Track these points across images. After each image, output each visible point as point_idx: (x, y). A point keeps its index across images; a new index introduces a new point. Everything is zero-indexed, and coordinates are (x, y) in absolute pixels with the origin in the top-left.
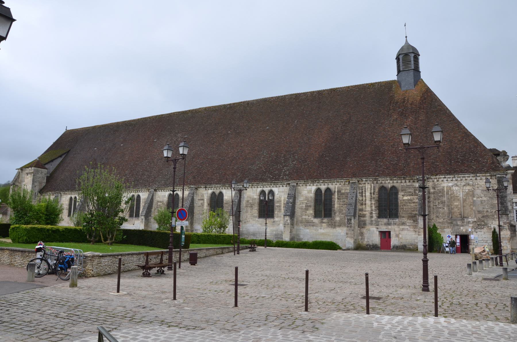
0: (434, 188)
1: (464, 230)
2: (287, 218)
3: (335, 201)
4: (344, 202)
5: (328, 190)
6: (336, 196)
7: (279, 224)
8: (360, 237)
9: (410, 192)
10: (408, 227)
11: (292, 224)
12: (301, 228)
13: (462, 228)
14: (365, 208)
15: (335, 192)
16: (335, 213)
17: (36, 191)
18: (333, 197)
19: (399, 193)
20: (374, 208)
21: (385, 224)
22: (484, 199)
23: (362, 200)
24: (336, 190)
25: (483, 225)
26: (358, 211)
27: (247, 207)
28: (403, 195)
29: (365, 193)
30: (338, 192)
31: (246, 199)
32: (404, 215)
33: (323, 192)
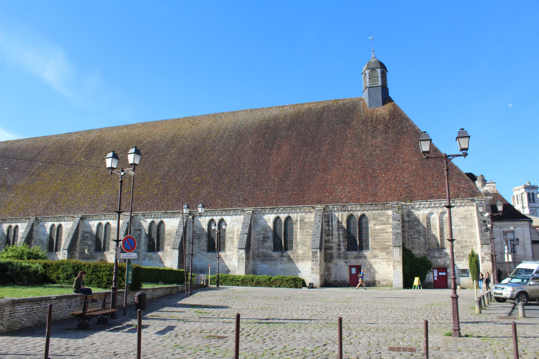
0: (408, 216)
1: (442, 263)
2: (243, 252)
3: (297, 232)
4: (308, 232)
5: (288, 218)
6: (299, 226)
7: (232, 259)
8: (327, 273)
9: (382, 221)
10: (380, 260)
11: (247, 258)
12: (258, 263)
13: (439, 260)
14: (332, 239)
15: (297, 221)
16: (297, 246)
18: (294, 226)
19: (371, 222)
20: (341, 239)
21: (355, 257)
22: (462, 227)
23: (329, 230)
24: (299, 219)
25: (462, 257)
26: (323, 242)
28: (374, 224)
29: (332, 222)
30: (300, 221)
32: (376, 247)
33: (283, 221)
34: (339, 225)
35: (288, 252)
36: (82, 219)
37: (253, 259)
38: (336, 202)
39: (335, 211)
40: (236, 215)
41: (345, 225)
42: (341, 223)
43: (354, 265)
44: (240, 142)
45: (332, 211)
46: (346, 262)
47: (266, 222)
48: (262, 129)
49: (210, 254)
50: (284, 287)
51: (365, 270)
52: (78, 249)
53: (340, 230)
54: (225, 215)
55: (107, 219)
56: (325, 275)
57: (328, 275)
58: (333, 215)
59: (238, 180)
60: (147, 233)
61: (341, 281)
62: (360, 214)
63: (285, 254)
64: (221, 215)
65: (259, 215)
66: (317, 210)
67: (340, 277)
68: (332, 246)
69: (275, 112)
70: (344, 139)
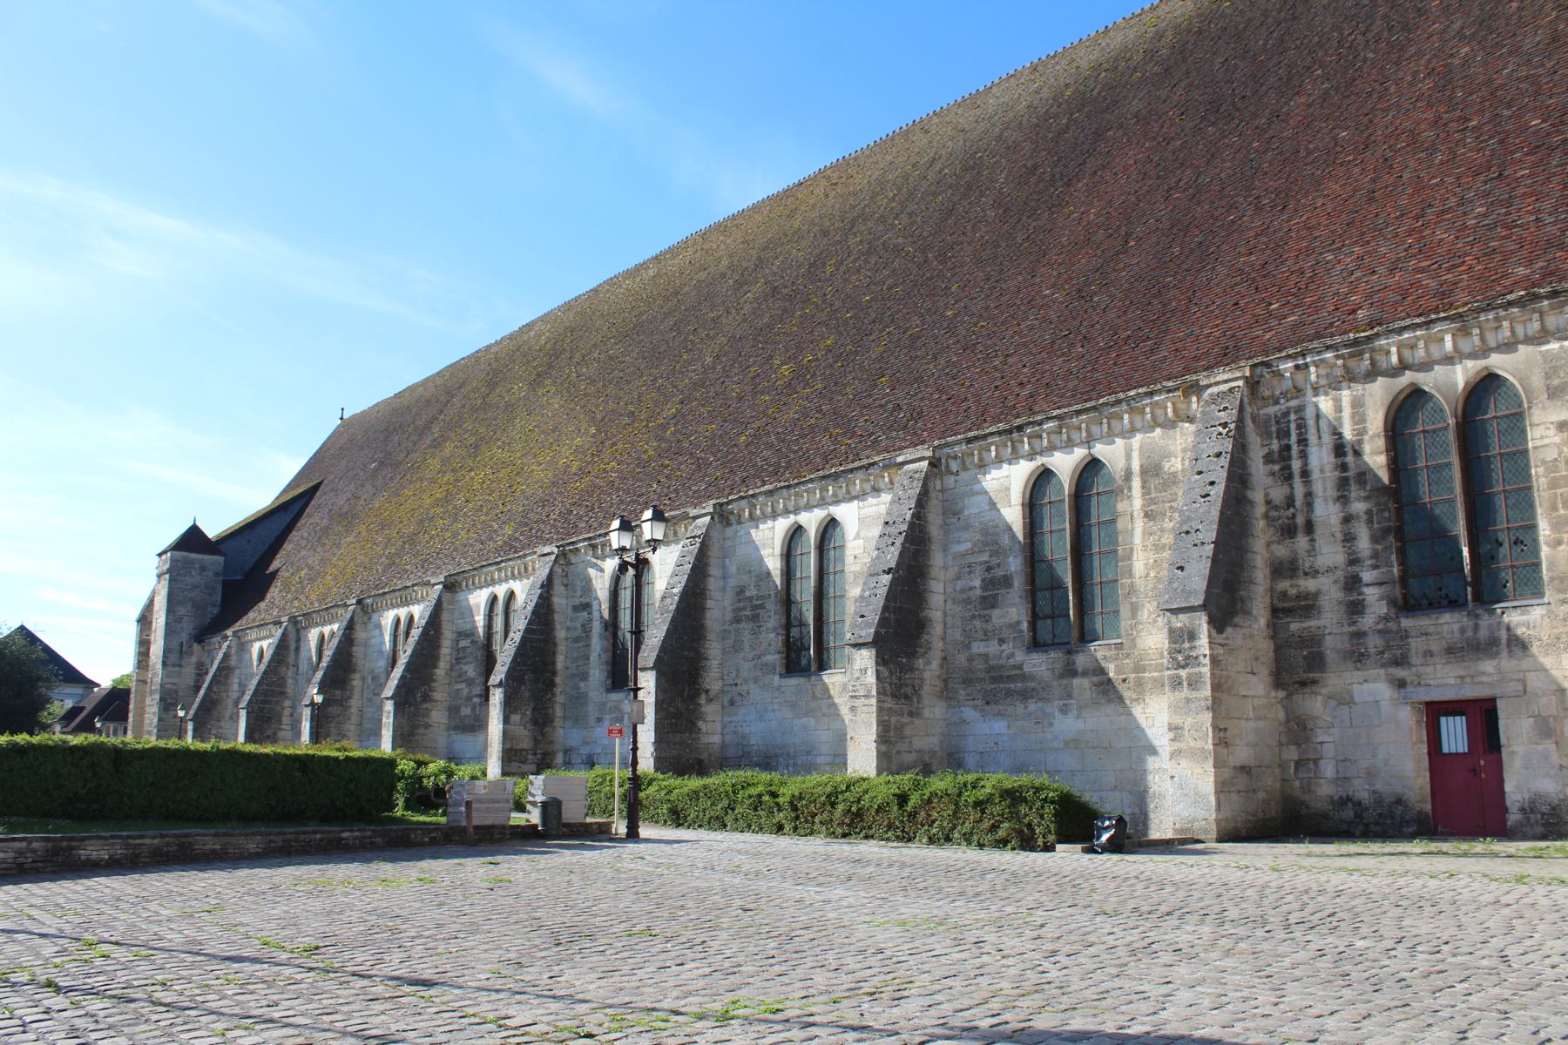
5: (1092, 467)
6: (1138, 502)
8: (1292, 754)
12: (969, 713)
14: (1312, 552)
15: (1128, 475)
16: (1135, 609)
17: (184, 637)
20: (1364, 544)
21: (1450, 651)
23: (1290, 501)
27: (737, 620)
29: (1304, 455)
31: (732, 582)
34: (1344, 467)
35: (1093, 646)
36: (451, 586)
37: (946, 692)
38: (1318, 336)
39: (1316, 390)
40: (876, 490)
41: (1376, 459)
42: (1357, 453)
43: (1449, 695)
44: (969, 188)
45: (1299, 391)
46: (1401, 684)
47: (993, 505)
48: (1057, 116)
49: (793, 681)
50: (967, 839)
51: (1526, 724)
52: (437, 696)
53: (1354, 492)
54: (837, 502)
55: (506, 580)
56: (1283, 766)
57: (1298, 764)
58: (1309, 413)
59: (914, 339)
60: (606, 614)
61: (1378, 799)
62: (1461, 375)
63: (1081, 660)
64: (823, 503)
65: (964, 475)
66: (1214, 399)
67: (1371, 774)
68: (1316, 595)
69: (1117, 40)
70: (1406, 28)
